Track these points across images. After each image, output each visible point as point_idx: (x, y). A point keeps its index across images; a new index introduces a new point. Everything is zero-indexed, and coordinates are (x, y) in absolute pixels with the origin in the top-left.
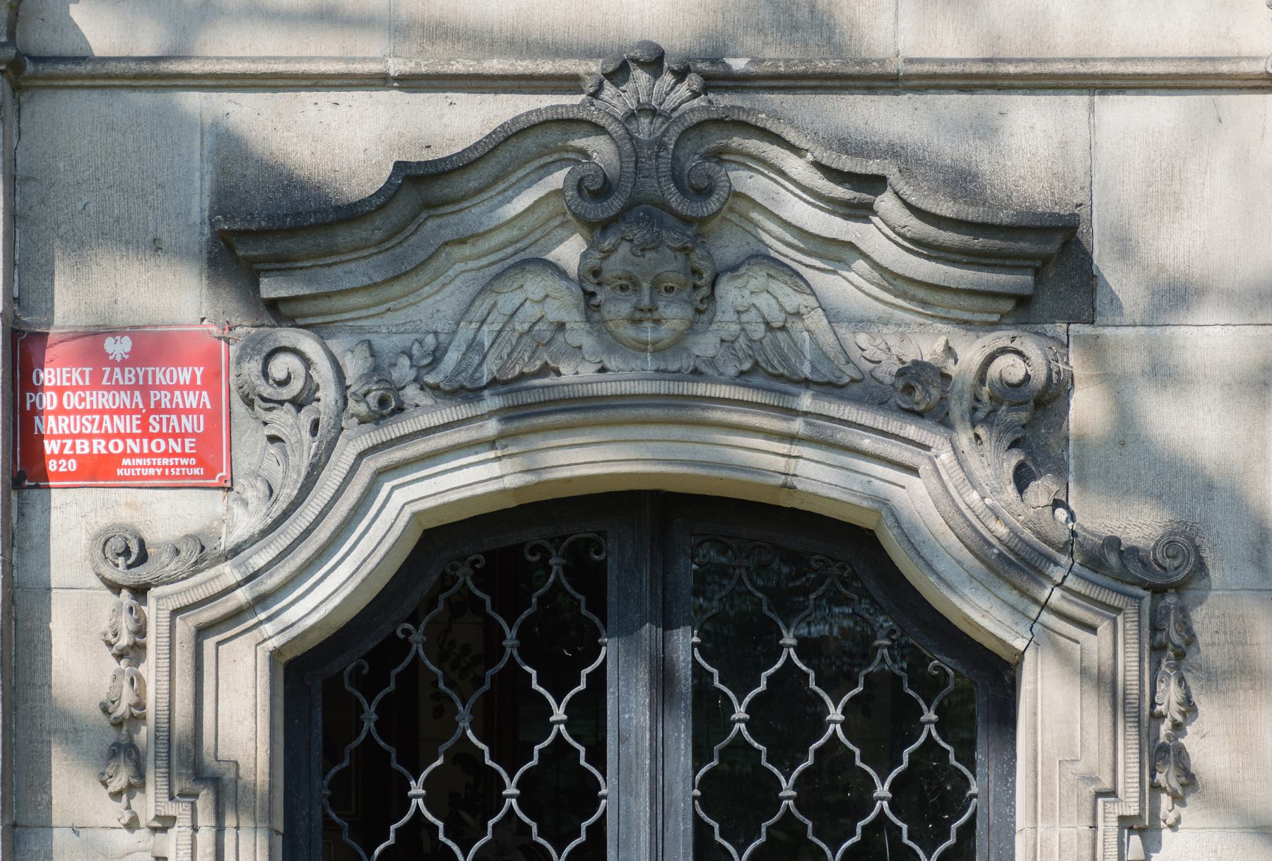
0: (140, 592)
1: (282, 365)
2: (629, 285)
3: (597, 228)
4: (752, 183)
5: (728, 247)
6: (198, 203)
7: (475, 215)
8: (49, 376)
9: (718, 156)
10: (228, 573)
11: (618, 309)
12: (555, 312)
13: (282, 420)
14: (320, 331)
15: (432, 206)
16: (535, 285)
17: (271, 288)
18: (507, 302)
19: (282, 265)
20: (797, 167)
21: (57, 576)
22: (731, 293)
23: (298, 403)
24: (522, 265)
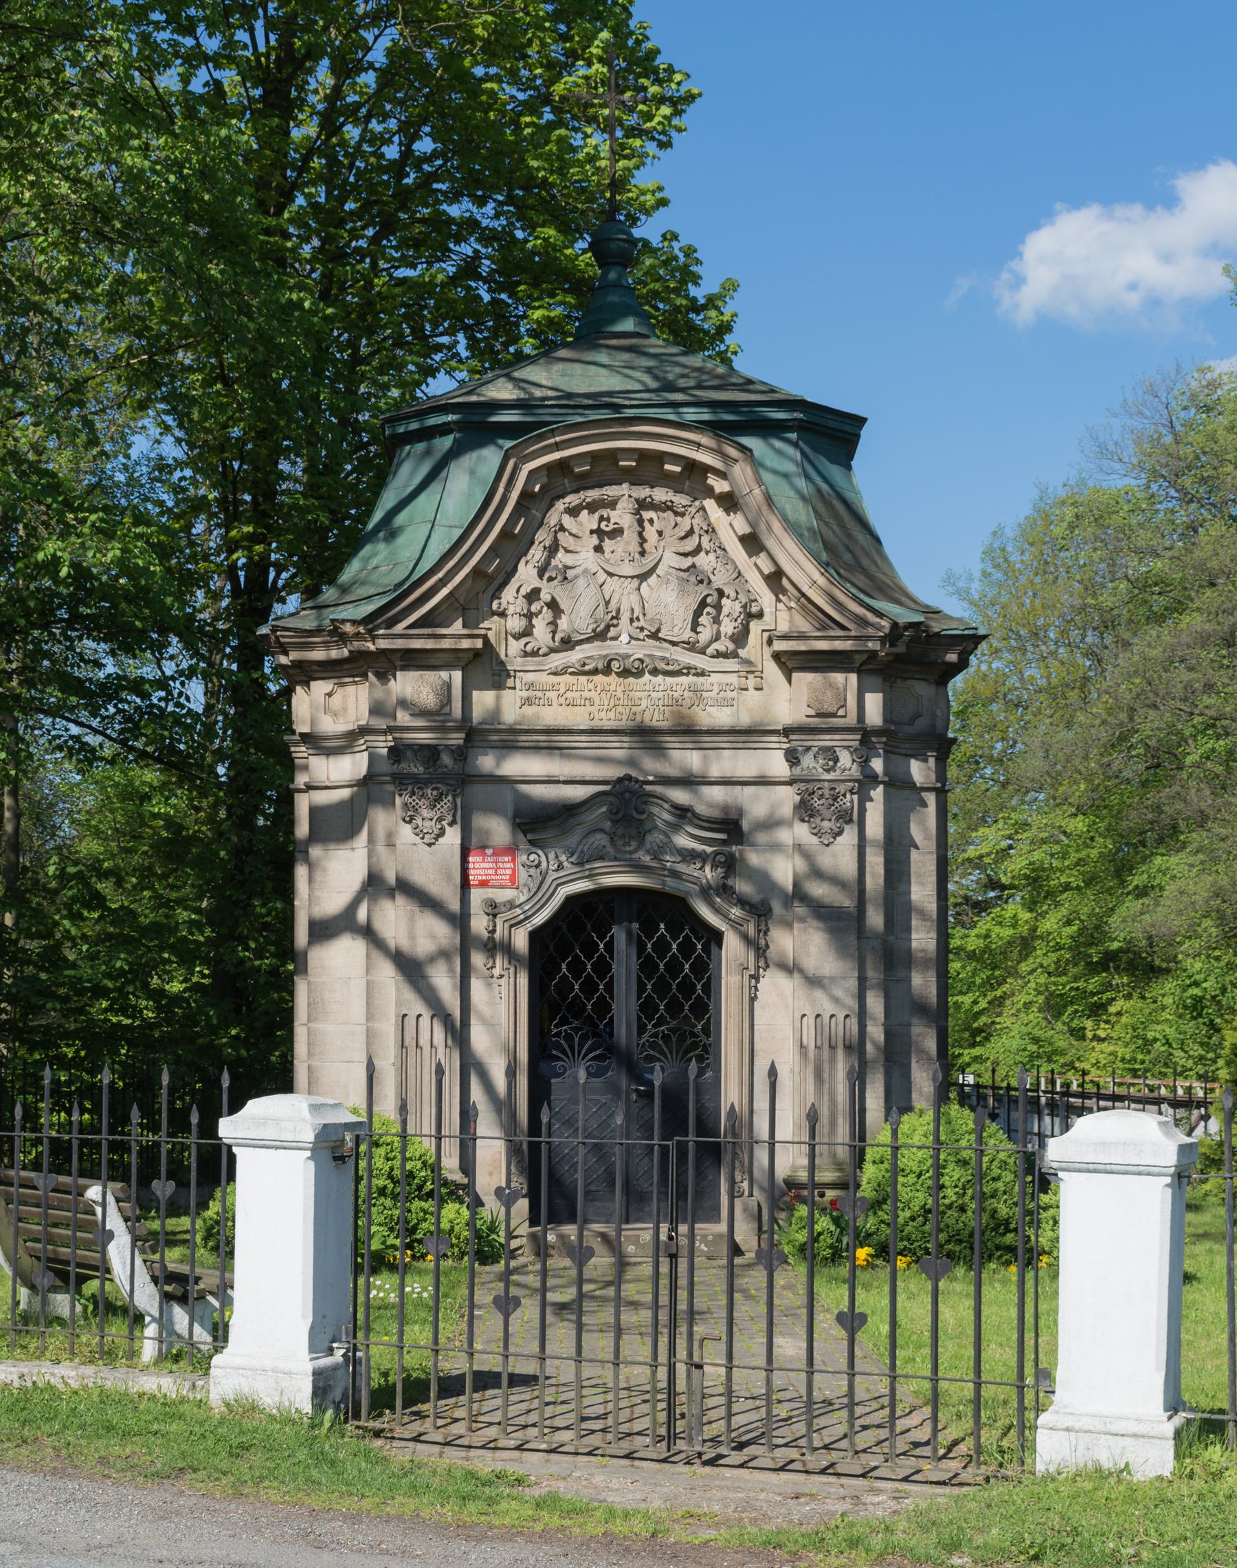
0: (495, 916)
1: (532, 857)
2: (623, 836)
3: (614, 822)
4: (656, 810)
5: (648, 826)
6: (510, 813)
7: (583, 818)
8: (471, 859)
9: (646, 803)
10: (518, 911)
11: (620, 843)
12: (603, 843)
13: (532, 871)
14: (542, 848)
15: (572, 816)
16: (598, 836)
17: (530, 837)
18: (591, 840)
19: (533, 831)
20: (666, 806)
21: (472, 911)
22: (649, 838)
23: (537, 866)
24: (595, 831)
